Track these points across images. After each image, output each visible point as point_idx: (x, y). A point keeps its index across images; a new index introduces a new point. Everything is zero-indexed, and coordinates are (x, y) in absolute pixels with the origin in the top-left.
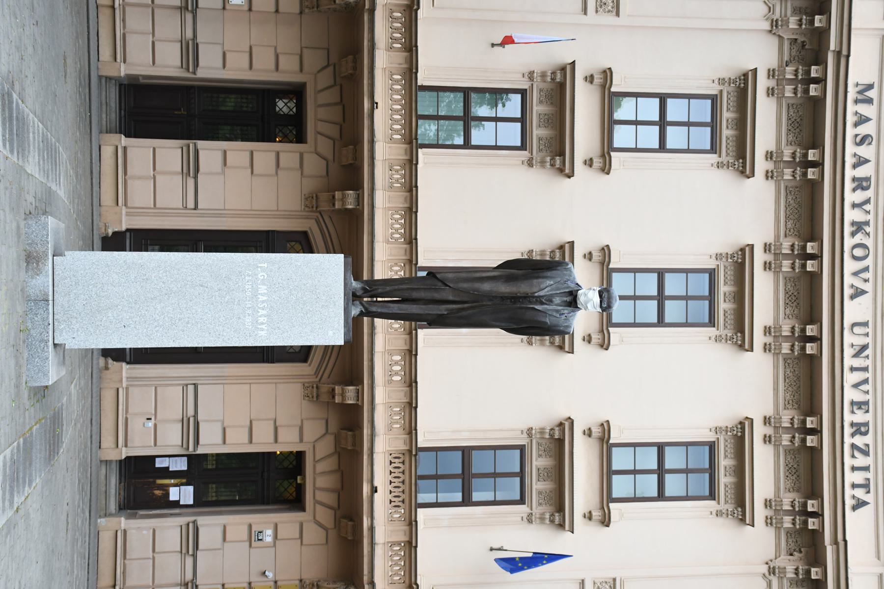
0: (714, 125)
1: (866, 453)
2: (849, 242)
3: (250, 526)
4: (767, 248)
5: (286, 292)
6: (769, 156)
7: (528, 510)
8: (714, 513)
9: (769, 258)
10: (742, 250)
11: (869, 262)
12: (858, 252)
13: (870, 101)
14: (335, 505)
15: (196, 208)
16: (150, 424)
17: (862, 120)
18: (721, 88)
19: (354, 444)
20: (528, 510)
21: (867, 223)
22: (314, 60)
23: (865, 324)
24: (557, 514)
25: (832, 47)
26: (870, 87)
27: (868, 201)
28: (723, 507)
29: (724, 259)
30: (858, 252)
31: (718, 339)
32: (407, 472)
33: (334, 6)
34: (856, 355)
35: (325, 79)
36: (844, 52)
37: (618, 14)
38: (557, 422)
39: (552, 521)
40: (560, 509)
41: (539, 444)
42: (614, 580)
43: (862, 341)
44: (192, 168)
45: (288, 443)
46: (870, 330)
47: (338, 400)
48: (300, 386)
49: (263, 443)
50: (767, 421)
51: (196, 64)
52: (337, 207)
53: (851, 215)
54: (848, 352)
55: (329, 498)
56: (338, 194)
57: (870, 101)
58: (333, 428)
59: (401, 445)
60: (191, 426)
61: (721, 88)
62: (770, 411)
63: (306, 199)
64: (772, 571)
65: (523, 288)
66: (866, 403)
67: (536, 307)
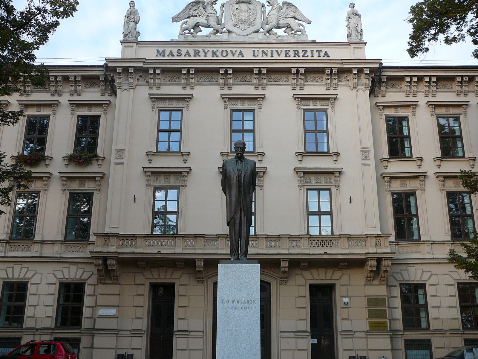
0: (171, 110)
1: (306, 51)
3: (342, 308)
4: (222, 89)
7: (334, 187)
8: (332, 110)
9: (226, 88)
10: (223, 98)
11: (228, 50)
12: (224, 54)
13: (164, 51)
14: (332, 270)
15: (203, 332)
17: (171, 53)
18: (156, 107)
19: (306, 262)
20: (334, 187)
21: (213, 51)
22: (140, 279)
23: (254, 51)
24: (335, 174)
25: (141, 65)
26: (158, 51)
27: (204, 51)
28: (330, 107)
29: (227, 105)
30: (224, 54)
31: (260, 108)
32: (318, 239)
33: (117, 270)
34: (267, 55)
35: (148, 274)
36: (144, 60)
37: (124, 150)
38: (296, 174)
39: (338, 177)
40: (332, 173)
41: (306, 182)
42: (361, 151)
43: (260, 53)
44: (186, 333)
45: (306, 291)
46: (256, 49)
47: (287, 270)
48: (281, 286)
49: (306, 302)
50: (294, 89)
51: (141, 330)
53: (209, 56)
54: (265, 57)
55: (330, 272)
56: (197, 269)
57: (164, 51)
58: (299, 271)
59: (306, 242)
61: (156, 107)
62: (290, 88)
63: (199, 283)
64: (355, 88)
65: (234, 181)
66: (286, 51)
67: (243, 176)
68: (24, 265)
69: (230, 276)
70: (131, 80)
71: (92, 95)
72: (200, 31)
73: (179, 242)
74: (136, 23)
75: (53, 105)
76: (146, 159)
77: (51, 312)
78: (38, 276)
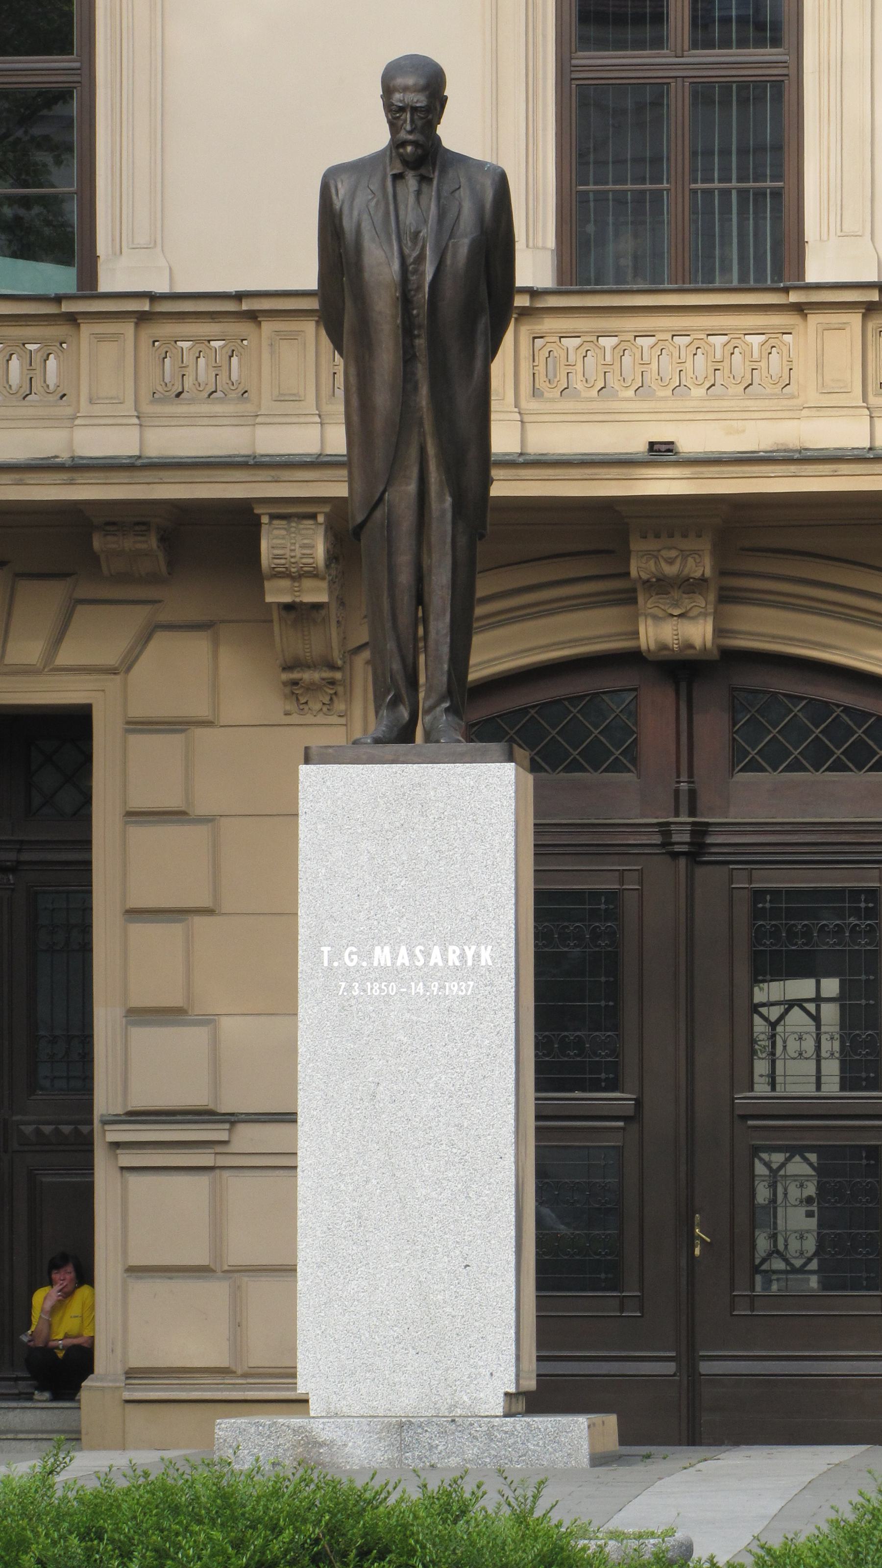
5: (388, 900)
52: (323, 598)
56: (277, 593)
63: (303, 707)
65: (383, 306)
67: (429, 277)
69: (363, 824)
73: (107, 358)
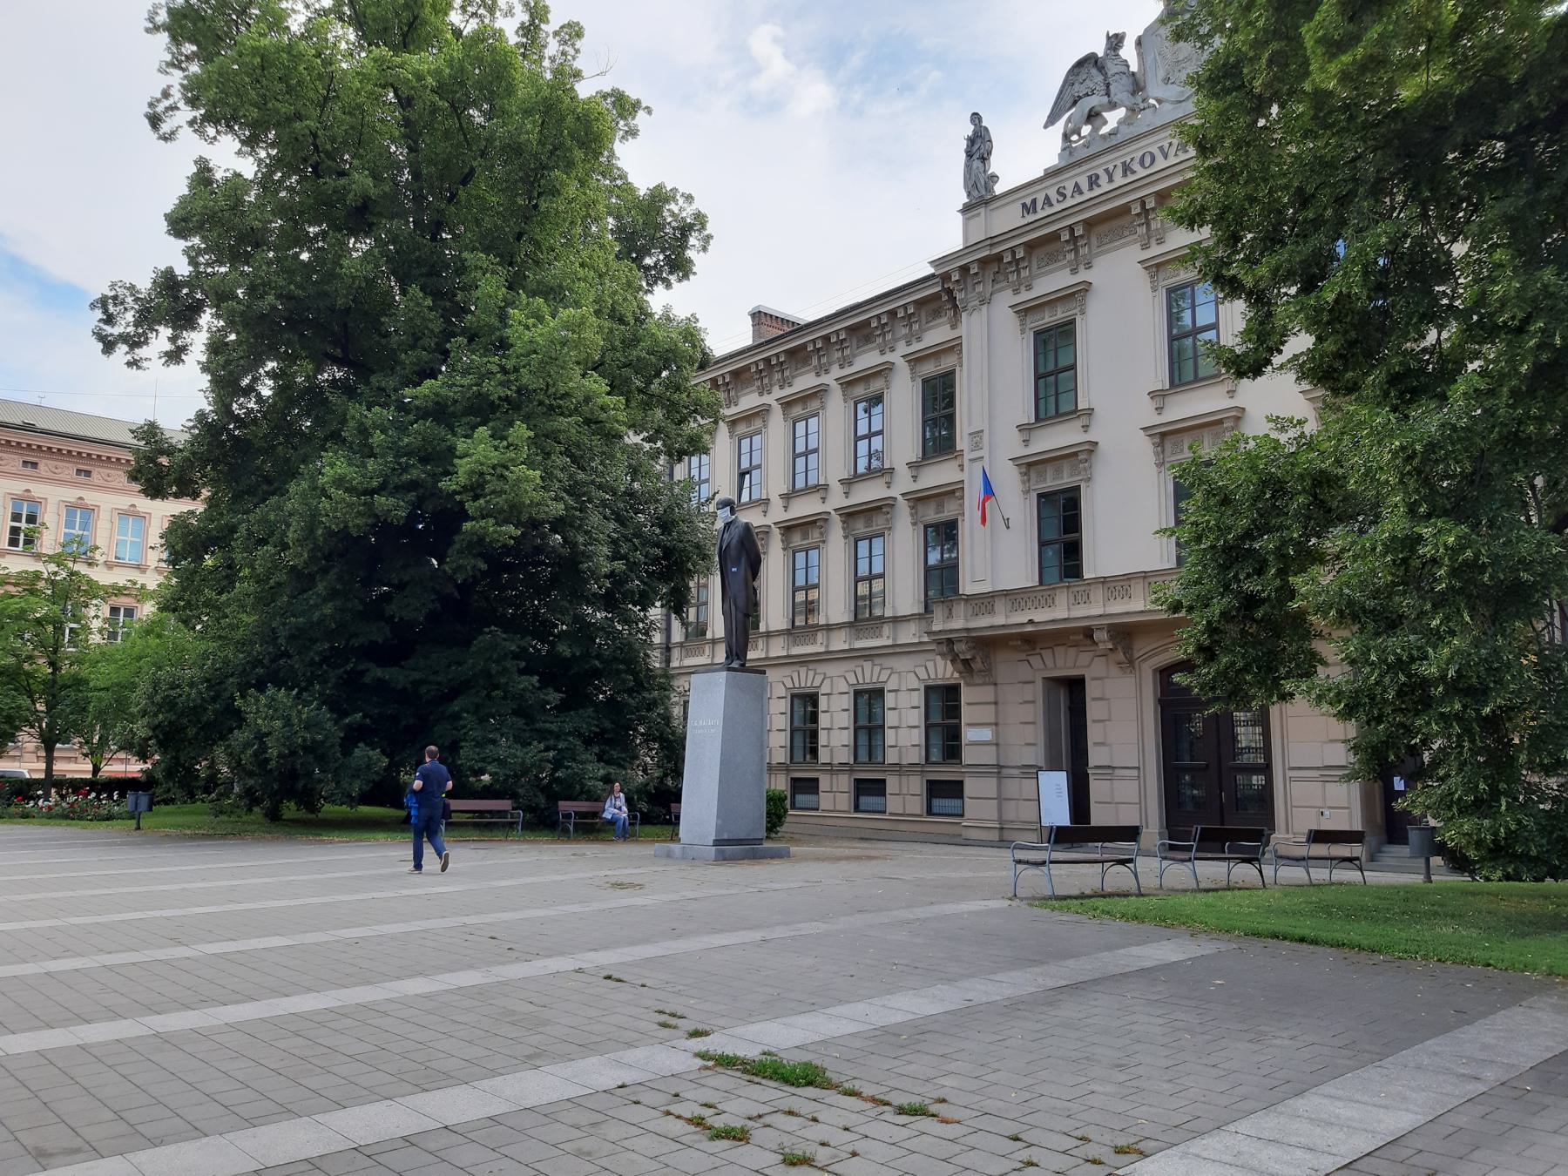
2: (1141, 173)
6: (1074, 271)
11: (1155, 150)
12: (1148, 160)
16: (1327, 812)
22: (1024, 671)
26: (1024, 205)
30: (1148, 160)
53: (1119, 180)
60: (1327, 771)
68: (877, 661)
70: (980, 288)
71: (937, 334)
72: (1105, 122)
74: (984, 159)
75: (884, 371)
76: (1150, 405)
77: (918, 737)
78: (895, 677)
